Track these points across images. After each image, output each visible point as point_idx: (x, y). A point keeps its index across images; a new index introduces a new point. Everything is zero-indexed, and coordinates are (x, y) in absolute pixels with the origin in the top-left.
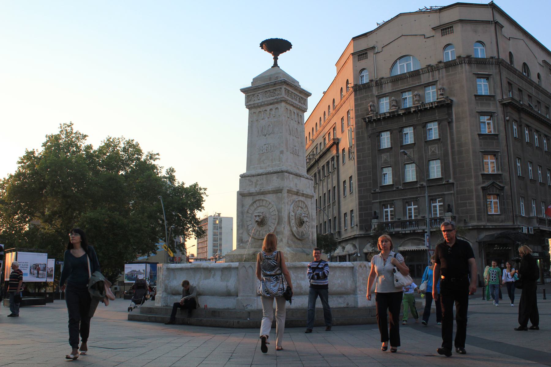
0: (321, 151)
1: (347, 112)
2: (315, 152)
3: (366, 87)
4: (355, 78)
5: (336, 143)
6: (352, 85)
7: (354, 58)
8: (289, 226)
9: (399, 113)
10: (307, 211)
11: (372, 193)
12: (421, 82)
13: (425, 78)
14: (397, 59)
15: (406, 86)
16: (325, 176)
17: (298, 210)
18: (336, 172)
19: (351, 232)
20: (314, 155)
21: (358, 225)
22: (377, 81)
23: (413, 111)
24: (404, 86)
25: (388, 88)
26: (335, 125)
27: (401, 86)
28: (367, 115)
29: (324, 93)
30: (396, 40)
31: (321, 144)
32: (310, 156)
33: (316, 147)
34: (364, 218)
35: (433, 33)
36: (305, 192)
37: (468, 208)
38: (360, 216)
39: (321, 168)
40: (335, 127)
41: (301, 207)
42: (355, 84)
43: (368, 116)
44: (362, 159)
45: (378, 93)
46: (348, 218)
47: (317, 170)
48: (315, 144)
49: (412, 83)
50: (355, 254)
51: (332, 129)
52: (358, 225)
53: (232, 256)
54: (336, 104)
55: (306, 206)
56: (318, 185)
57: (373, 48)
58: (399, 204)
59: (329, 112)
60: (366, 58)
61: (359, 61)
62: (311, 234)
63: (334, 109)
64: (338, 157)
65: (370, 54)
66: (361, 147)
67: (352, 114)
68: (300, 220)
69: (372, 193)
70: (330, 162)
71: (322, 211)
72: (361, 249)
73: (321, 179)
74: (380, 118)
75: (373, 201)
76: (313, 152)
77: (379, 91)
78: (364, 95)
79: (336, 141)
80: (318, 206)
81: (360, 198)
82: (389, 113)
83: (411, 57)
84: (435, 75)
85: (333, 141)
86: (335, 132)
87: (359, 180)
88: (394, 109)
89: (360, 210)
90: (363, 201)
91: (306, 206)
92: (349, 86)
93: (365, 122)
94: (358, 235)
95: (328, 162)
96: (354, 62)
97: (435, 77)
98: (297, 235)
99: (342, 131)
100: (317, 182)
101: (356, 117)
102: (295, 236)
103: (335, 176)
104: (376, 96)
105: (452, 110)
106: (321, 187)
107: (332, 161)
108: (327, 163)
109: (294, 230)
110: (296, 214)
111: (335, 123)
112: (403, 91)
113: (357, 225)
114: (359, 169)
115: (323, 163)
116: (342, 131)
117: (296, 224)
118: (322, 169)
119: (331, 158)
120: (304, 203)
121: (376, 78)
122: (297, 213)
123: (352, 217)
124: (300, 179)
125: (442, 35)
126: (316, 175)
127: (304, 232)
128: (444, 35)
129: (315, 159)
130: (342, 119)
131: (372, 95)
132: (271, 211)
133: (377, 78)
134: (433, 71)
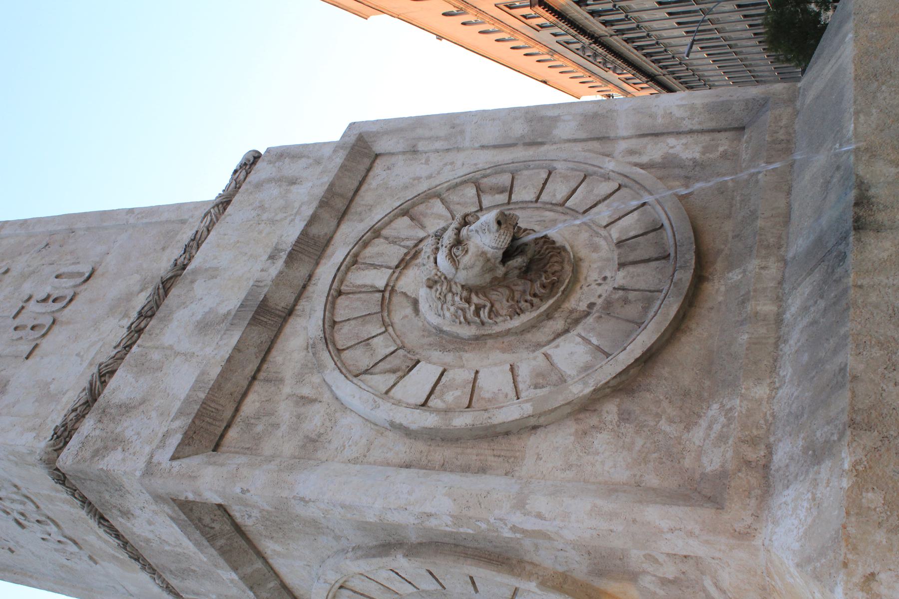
0: (567, 33)
2: (579, 46)
8: (534, 443)
10: (453, 197)
16: (627, 16)
17: (415, 303)
20: (583, 48)
26: (501, 6)
29: (440, 37)
31: (555, 35)
32: (589, 56)
33: (566, 45)
36: (291, 233)
39: (609, 30)
40: (506, 6)
41: (404, 264)
47: (616, 37)
51: (513, 11)
54: (455, 10)
55: (404, 212)
56: (651, 33)
59: (476, 23)
62: (655, 151)
63: (461, 12)
68: (497, 283)
70: (589, 8)
71: (708, 17)
73: (634, 26)
76: (578, 49)
80: (695, 29)
85: (537, 7)
86: (518, 4)
91: (405, 213)
95: (593, 13)
98: (639, 324)
100: (645, 34)
102: (649, 358)
106: (655, 25)
107: (588, 5)
108: (594, 17)
109: (587, 368)
110: (440, 331)
117: (533, 326)
118: (612, 25)
119: (580, 6)
120: (376, 233)
122: (434, 320)
124: (194, 272)
126: (629, 39)
127: (631, 224)
129: (590, 44)
132: (411, 589)
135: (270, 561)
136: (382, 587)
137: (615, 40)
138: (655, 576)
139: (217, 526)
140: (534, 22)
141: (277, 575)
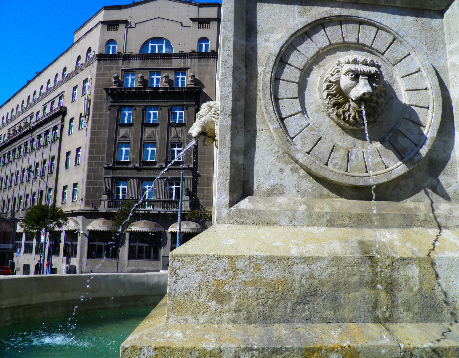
1: (84, 81)
3: (115, 57)
4: (100, 47)
5: (63, 112)
6: (97, 53)
7: (102, 27)
9: (146, 91)
11: (105, 168)
12: (172, 66)
13: (177, 63)
14: (150, 39)
15: (156, 66)
18: (58, 142)
19: (72, 206)
21: (84, 200)
22: (125, 55)
23: (161, 91)
24: (153, 66)
25: (135, 64)
27: (150, 64)
28: (111, 86)
30: (151, 21)
34: (91, 193)
35: (190, 23)
37: (205, 194)
38: (88, 190)
40: (62, 95)
42: (100, 52)
43: (111, 87)
44: (96, 130)
45: (124, 67)
46: (69, 192)
47: (30, 138)
48: (29, 112)
49: (161, 64)
50: (76, 230)
52: (84, 200)
53: (224, 264)
54: (66, 73)
57: (126, 22)
58: (134, 183)
60: (116, 30)
61: (107, 30)
64: (62, 127)
65: (122, 27)
66: (98, 118)
67: (91, 84)
69: (105, 168)
70: (51, 131)
72: (84, 226)
74: (124, 92)
75: (105, 176)
77: (126, 66)
78: (109, 65)
79: (64, 110)
81: (89, 171)
82: (136, 89)
83: (165, 41)
84: (187, 62)
85: (59, 109)
87: (91, 152)
88: (140, 86)
89: (89, 183)
90: (92, 174)
92: (92, 53)
93: (107, 93)
94: (83, 210)
96: (102, 30)
97: (187, 64)
99: (73, 100)
101: (96, 86)
103: (55, 147)
104: (122, 70)
105: (199, 99)
107: (53, 131)
111: (64, 92)
112: (152, 71)
113: (82, 200)
114: (92, 140)
115: (36, 133)
116: (73, 100)
121: (124, 51)
123: (74, 191)
125: (199, 28)
128: (201, 28)
129: (30, 127)
130: (75, 88)
131: (117, 68)
133: (125, 52)
134: (186, 58)
136: (400, 59)
137: (28, 138)
138: (437, 184)
140: (49, 106)
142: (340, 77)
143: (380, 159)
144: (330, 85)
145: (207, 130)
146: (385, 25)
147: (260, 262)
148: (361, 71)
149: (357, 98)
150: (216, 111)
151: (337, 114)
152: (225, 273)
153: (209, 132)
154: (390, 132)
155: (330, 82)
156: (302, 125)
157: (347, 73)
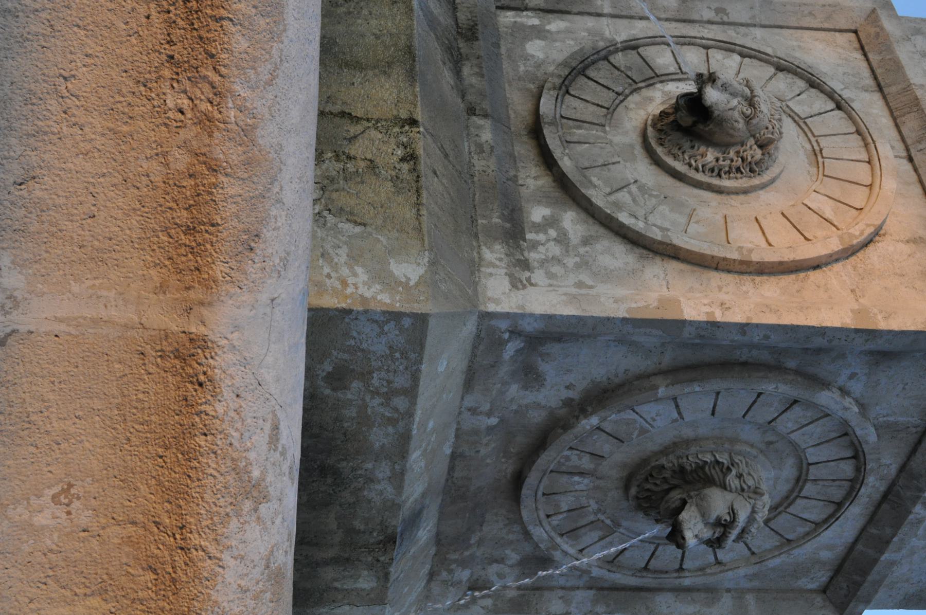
135: (851, 540)
139: (844, 585)
141: (863, 530)
142: (731, 491)
143: (566, 508)
144: (723, 466)
145: (711, 126)
146: (819, 534)
147: (401, 424)
148: (730, 533)
149: (680, 524)
150: (750, 163)
151: (663, 467)
152: (385, 383)
153: (707, 129)
154: (612, 521)
155: (729, 469)
156: (654, 420)
157: (733, 512)
